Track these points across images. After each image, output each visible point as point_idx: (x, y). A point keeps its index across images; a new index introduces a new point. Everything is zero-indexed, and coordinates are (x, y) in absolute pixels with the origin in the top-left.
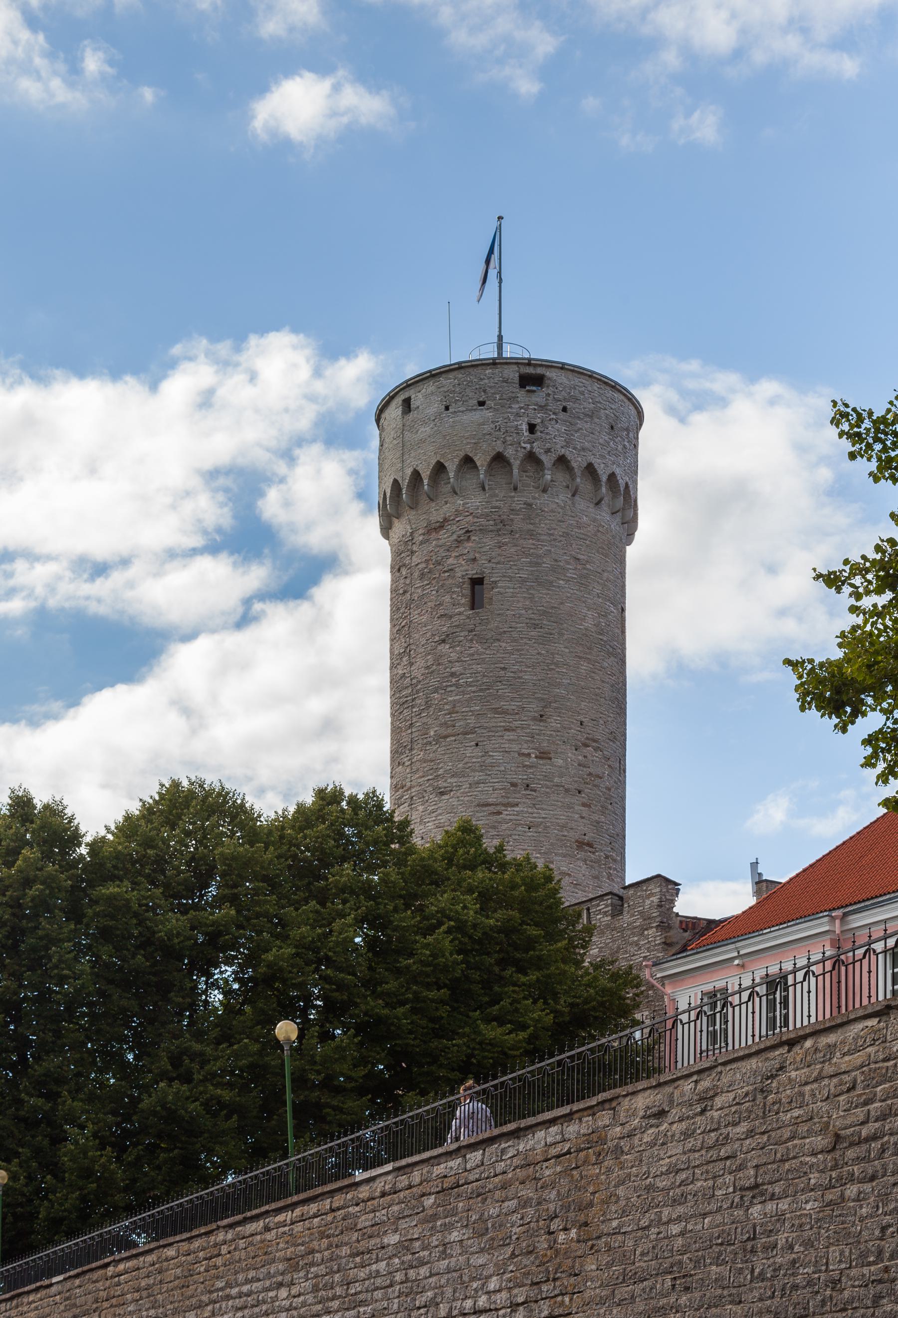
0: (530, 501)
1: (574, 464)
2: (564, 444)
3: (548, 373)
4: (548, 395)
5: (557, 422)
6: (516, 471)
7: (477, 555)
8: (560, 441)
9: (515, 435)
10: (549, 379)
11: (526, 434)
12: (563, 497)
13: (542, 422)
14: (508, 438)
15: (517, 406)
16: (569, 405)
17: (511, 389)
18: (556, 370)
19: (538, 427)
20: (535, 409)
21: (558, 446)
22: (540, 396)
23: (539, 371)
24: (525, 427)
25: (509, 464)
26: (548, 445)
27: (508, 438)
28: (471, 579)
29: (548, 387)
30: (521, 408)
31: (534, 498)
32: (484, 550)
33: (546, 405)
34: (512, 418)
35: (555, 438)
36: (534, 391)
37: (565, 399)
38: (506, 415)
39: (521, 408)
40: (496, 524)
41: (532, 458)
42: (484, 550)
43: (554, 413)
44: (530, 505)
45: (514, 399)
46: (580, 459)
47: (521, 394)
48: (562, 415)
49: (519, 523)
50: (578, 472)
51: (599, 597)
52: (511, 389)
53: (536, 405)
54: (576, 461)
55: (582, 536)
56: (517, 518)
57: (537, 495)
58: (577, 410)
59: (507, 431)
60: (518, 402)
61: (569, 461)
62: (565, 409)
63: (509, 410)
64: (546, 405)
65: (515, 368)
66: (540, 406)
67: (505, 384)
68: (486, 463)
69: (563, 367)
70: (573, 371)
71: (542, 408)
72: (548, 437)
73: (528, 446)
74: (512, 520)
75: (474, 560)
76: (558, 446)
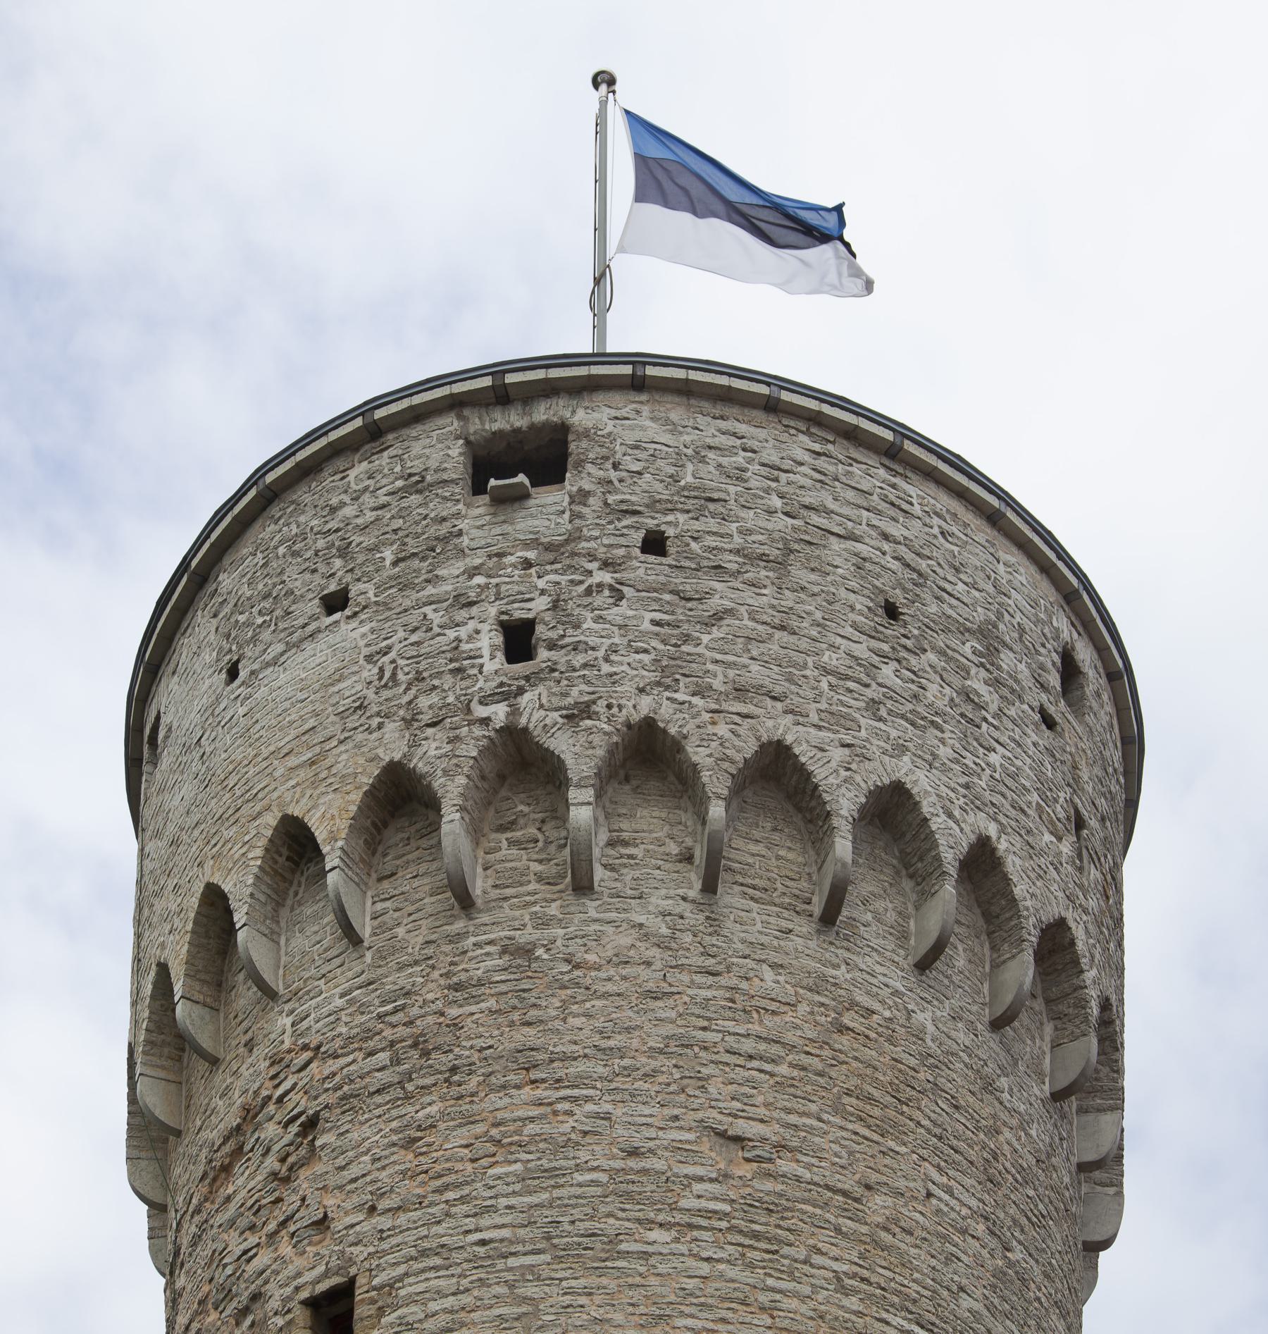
0: (524, 937)
1: (698, 754)
2: (652, 676)
3: (581, 415)
4: (581, 497)
5: (619, 597)
6: (452, 823)
7: (330, 1201)
8: (634, 668)
9: (448, 681)
10: (586, 434)
11: (494, 664)
12: (667, 895)
13: (555, 606)
14: (424, 702)
15: (457, 567)
16: (674, 525)
17: (437, 508)
18: (617, 398)
19: (540, 629)
20: (527, 564)
21: (628, 687)
22: (547, 510)
23: (542, 413)
24: (489, 641)
25: (432, 804)
26: (578, 693)
27: (424, 702)
28: (305, 1303)
29: (580, 464)
30: (472, 573)
31: (543, 922)
32: (355, 1170)
33: (574, 537)
34: (436, 618)
35: (616, 663)
36: (520, 496)
37: (653, 504)
38: (414, 618)
39: (472, 573)
40: (396, 1061)
41: (521, 766)
42: (355, 1170)
43: (606, 565)
44: (526, 951)
45: (445, 544)
46: (722, 730)
47: (474, 520)
48: (644, 569)
49: (480, 1026)
50: (716, 783)
51: (846, 1292)
52: (437, 508)
53: (534, 543)
54: (705, 740)
55: (748, 1046)
56: (473, 1014)
57: (554, 909)
58: (711, 541)
59: (419, 678)
60: (461, 552)
61: (677, 746)
62: (655, 544)
63: (430, 590)
64: (574, 537)
65: (450, 423)
66: (549, 548)
67: (415, 499)
68: (343, 825)
69: (641, 378)
70: (685, 390)
71: (555, 551)
72: (579, 660)
73: (499, 712)
74: (455, 1025)
75: (322, 1224)
76: (628, 687)
